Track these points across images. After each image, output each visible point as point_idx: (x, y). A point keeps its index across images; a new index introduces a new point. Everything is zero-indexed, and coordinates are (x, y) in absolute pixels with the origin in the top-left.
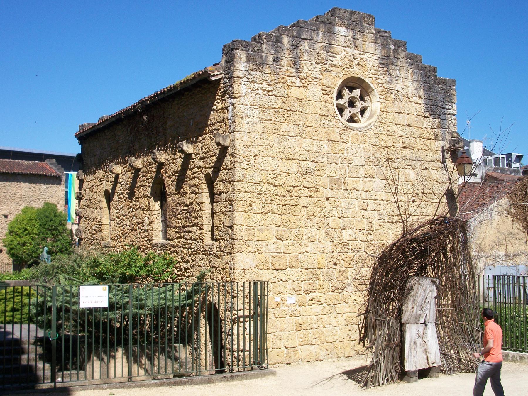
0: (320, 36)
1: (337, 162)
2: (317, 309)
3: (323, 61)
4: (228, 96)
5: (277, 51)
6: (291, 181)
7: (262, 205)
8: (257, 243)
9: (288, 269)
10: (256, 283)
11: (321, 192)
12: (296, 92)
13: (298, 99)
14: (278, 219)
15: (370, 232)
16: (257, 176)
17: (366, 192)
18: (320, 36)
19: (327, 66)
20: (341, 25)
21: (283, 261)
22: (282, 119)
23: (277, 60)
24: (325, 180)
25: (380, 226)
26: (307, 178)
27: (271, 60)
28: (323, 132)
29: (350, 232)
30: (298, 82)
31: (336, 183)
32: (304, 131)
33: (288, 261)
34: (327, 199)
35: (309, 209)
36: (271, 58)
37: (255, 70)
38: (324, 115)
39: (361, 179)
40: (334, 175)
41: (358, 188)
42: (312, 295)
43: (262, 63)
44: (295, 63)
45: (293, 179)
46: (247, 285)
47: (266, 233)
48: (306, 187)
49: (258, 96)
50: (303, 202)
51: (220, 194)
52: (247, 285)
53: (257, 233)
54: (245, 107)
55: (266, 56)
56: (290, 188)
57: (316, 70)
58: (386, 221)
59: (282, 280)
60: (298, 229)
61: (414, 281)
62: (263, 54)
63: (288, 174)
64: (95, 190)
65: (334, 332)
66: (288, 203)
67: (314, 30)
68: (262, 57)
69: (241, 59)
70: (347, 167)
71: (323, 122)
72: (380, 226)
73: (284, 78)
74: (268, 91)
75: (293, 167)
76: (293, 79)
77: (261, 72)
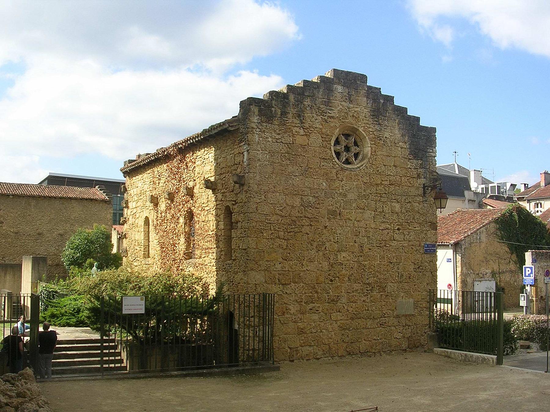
0: (321, 93)
1: (333, 197)
2: (316, 317)
3: (323, 113)
4: (244, 143)
5: (284, 106)
6: (295, 213)
7: (270, 232)
8: (266, 263)
9: (292, 284)
10: (264, 295)
11: (320, 221)
12: (300, 140)
13: (301, 145)
14: (284, 243)
15: (361, 254)
16: (266, 209)
17: (358, 221)
18: (321, 93)
19: (326, 118)
20: (339, 84)
21: (288, 278)
22: (288, 162)
23: (284, 113)
24: (324, 212)
25: (370, 249)
26: (308, 210)
27: (279, 113)
28: (322, 173)
29: (344, 254)
30: (302, 132)
31: (333, 214)
32: (306, 172)
33: (292, 277)
34: (326, 227)
35: (310, 236)
36: (279, 112)
37: (266, 122)
38: (324, 158)
39: (353, 211)
40: (331, 207)
41: (351, 218)
42: (311, 306)
43: (273, 117)
44: (299, 116)
45: (297, 211)
46: (257, 297)
47: (274, 255)
48: (308, 218)
49: (268, 143)
50: (306, 229)
51: (237, 223)
52: (257, 297)
53: (266, 255)
54: (258, 152)
55: (275, 110)
56: (294, 218)
57: (317, 121)
58: (375, 245)
59: (286, 293)
60: (300, 252)
61: (124, 312)
62: (273, 109)
63: (293, 207)
64: (137, 216)
65: (330, 336)
66: (292, 230)
67: (315, 88)
68: (271, 111)
69: (254, 113)
70: (342, 201)
71: (322, 164)
72: (370, 249)
73: (290, 128)
74: (277, 139)
75: (297, 202)
76: (298, 129)
77: (271, 123)
